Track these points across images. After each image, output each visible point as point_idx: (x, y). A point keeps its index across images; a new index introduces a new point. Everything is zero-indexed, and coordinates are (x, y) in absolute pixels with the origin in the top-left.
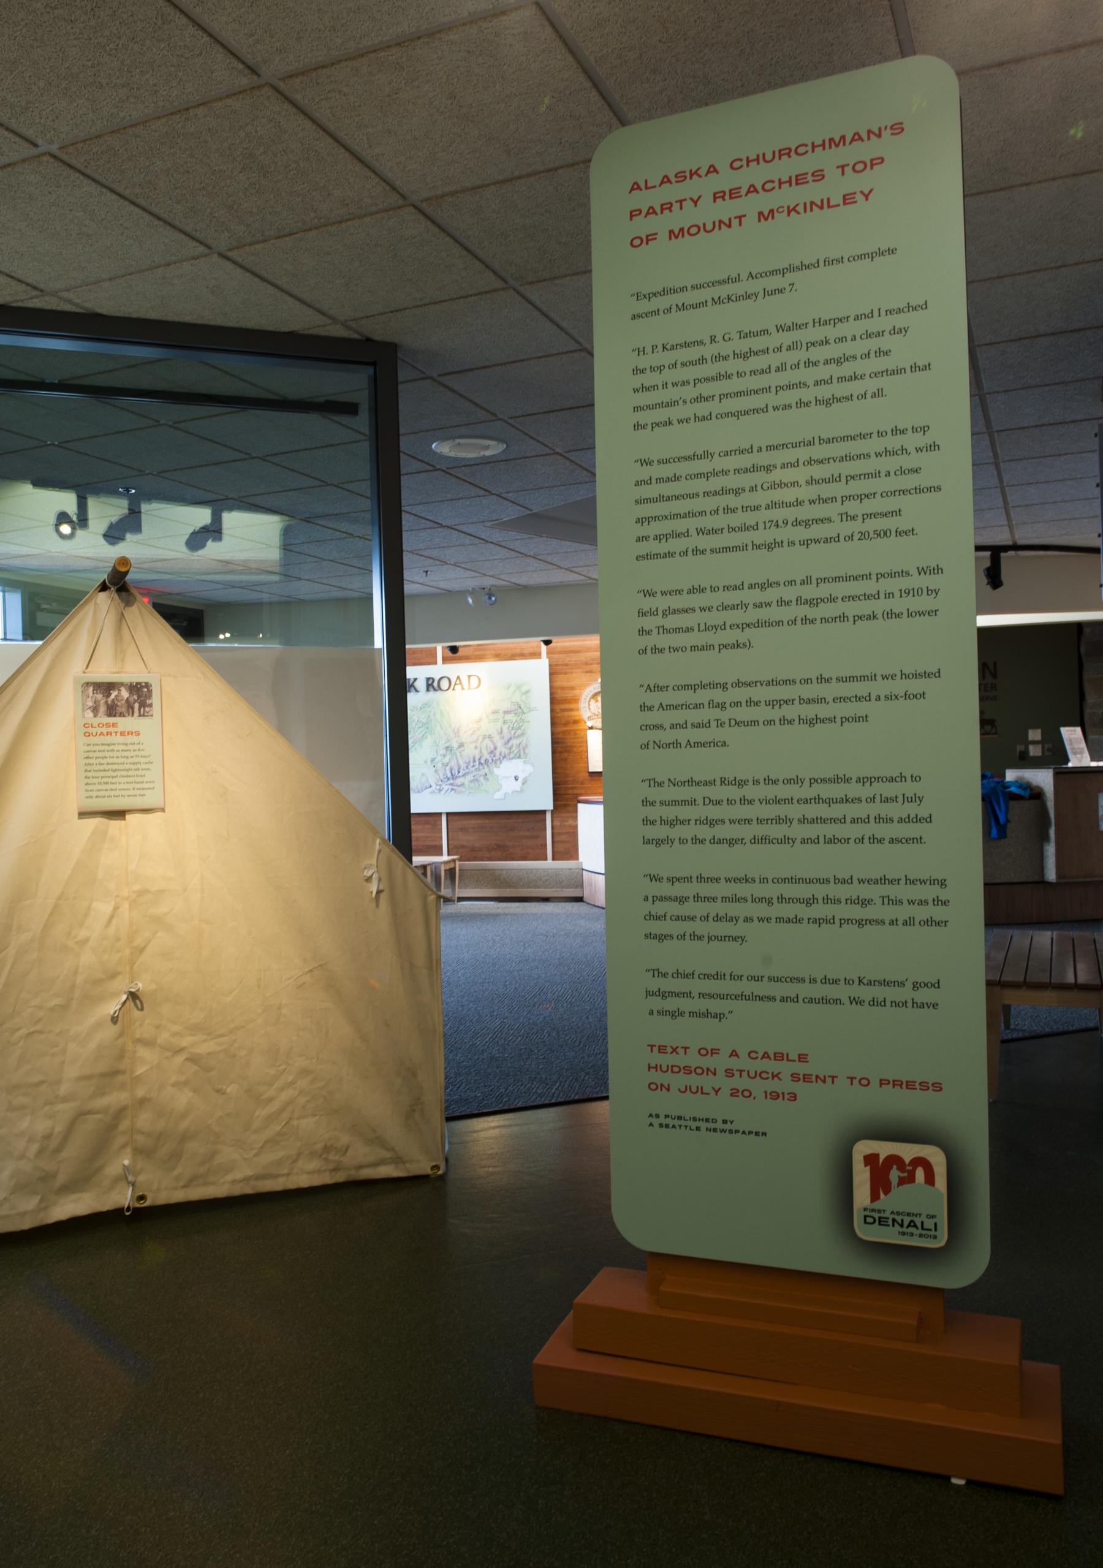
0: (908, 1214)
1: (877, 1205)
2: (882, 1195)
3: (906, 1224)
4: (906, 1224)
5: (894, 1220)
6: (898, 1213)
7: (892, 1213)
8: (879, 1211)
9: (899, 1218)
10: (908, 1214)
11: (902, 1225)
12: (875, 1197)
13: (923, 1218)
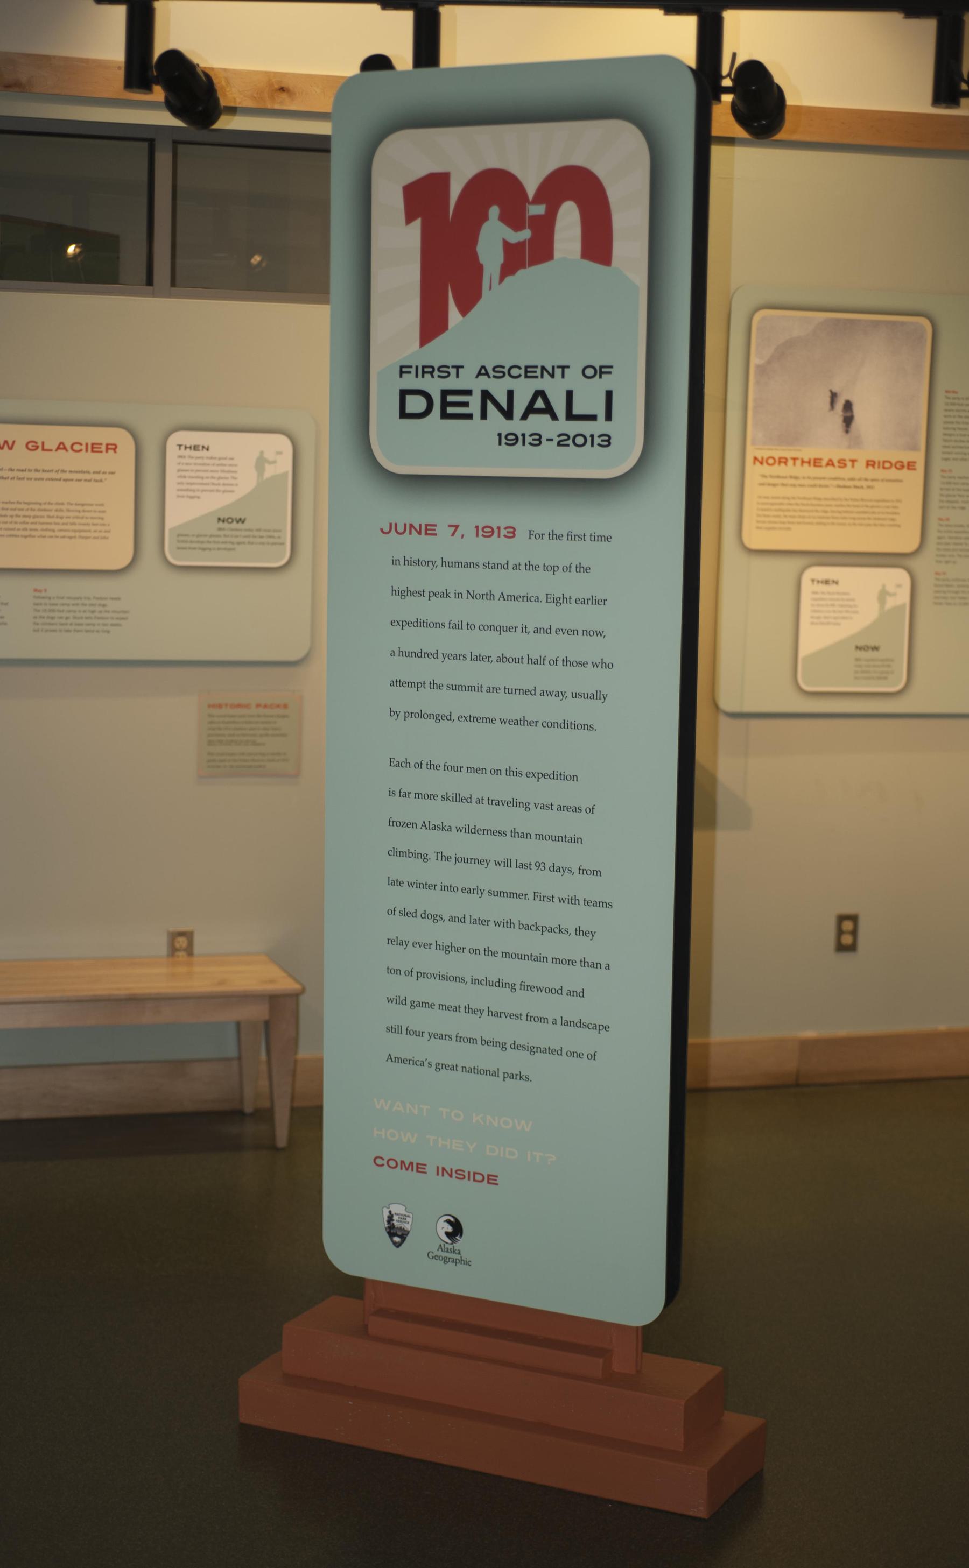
0: (529, 372)
1: (440, 351)
2: (454, 314)
3: (519, 407)
4: (519, 407)
5: (486, 396)
6: (500, 372)
7: (482, 372)
8: (444, 372)
9: (499, 390)
10: (529, 372)
11: (508, 414)
12: (432, 325)
13: (573, 380)
